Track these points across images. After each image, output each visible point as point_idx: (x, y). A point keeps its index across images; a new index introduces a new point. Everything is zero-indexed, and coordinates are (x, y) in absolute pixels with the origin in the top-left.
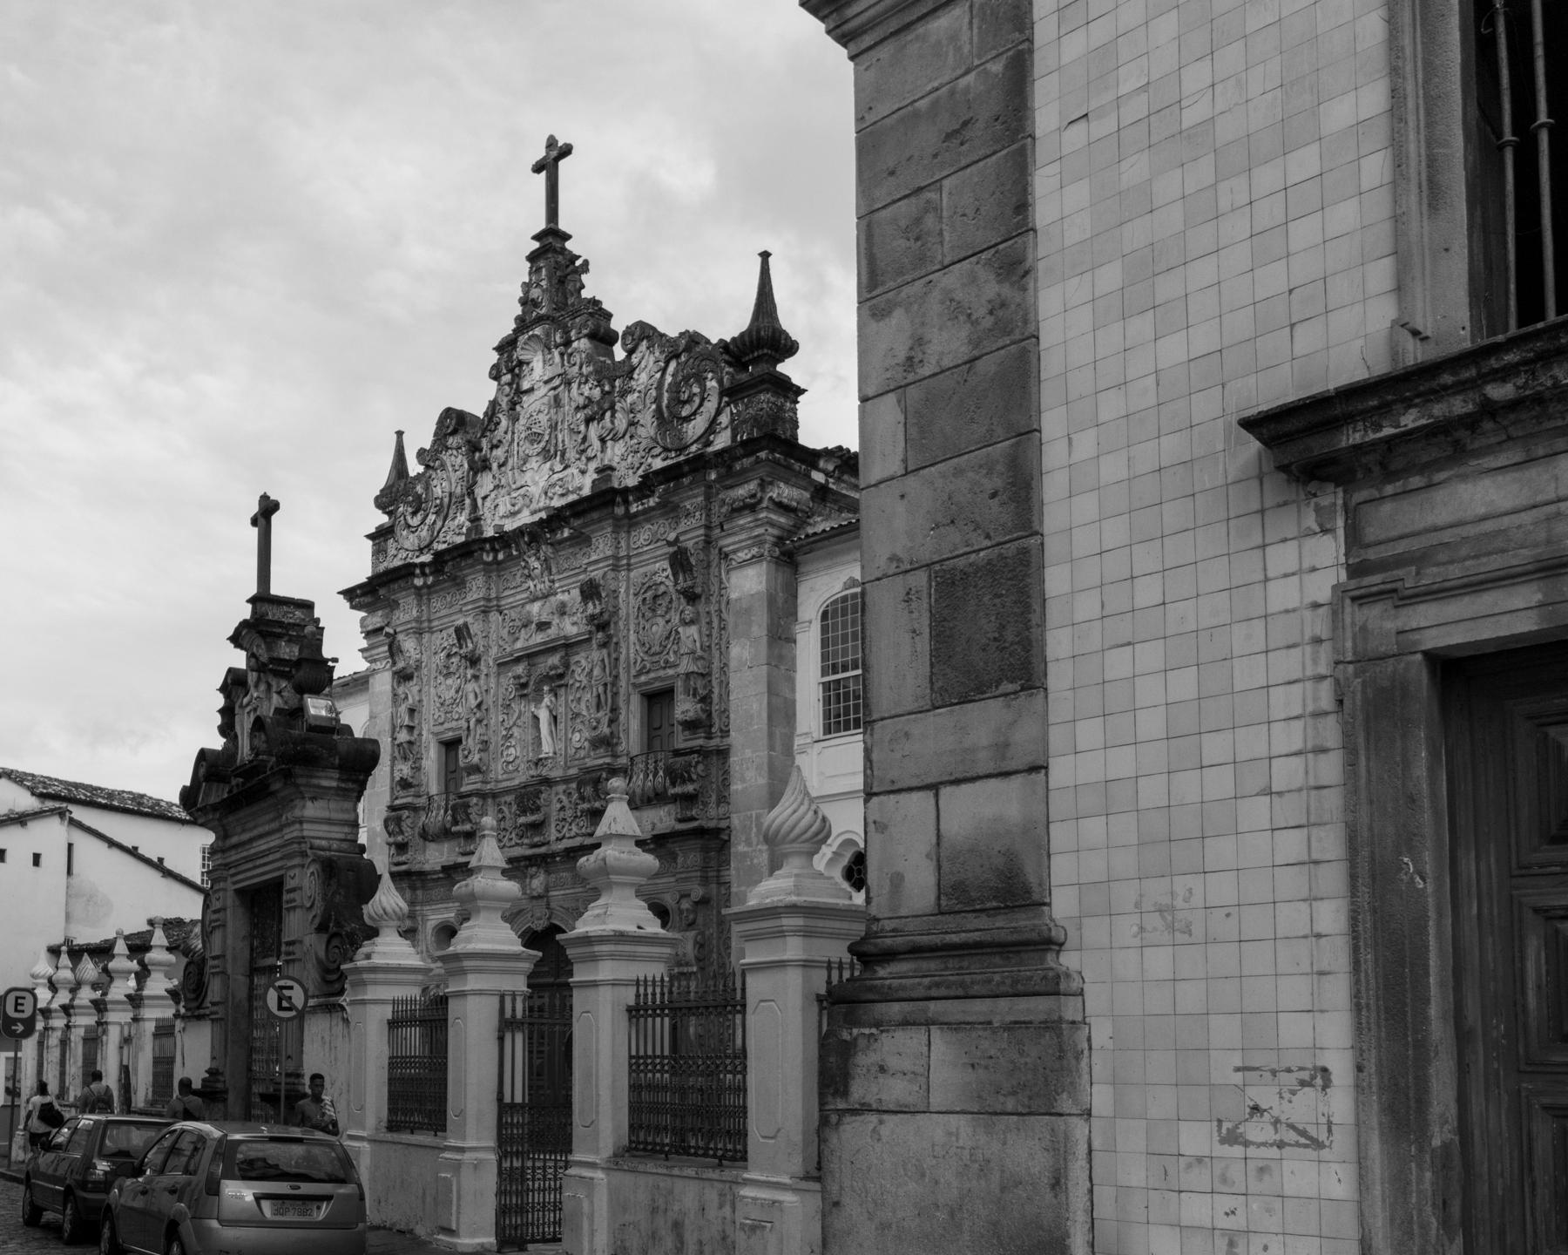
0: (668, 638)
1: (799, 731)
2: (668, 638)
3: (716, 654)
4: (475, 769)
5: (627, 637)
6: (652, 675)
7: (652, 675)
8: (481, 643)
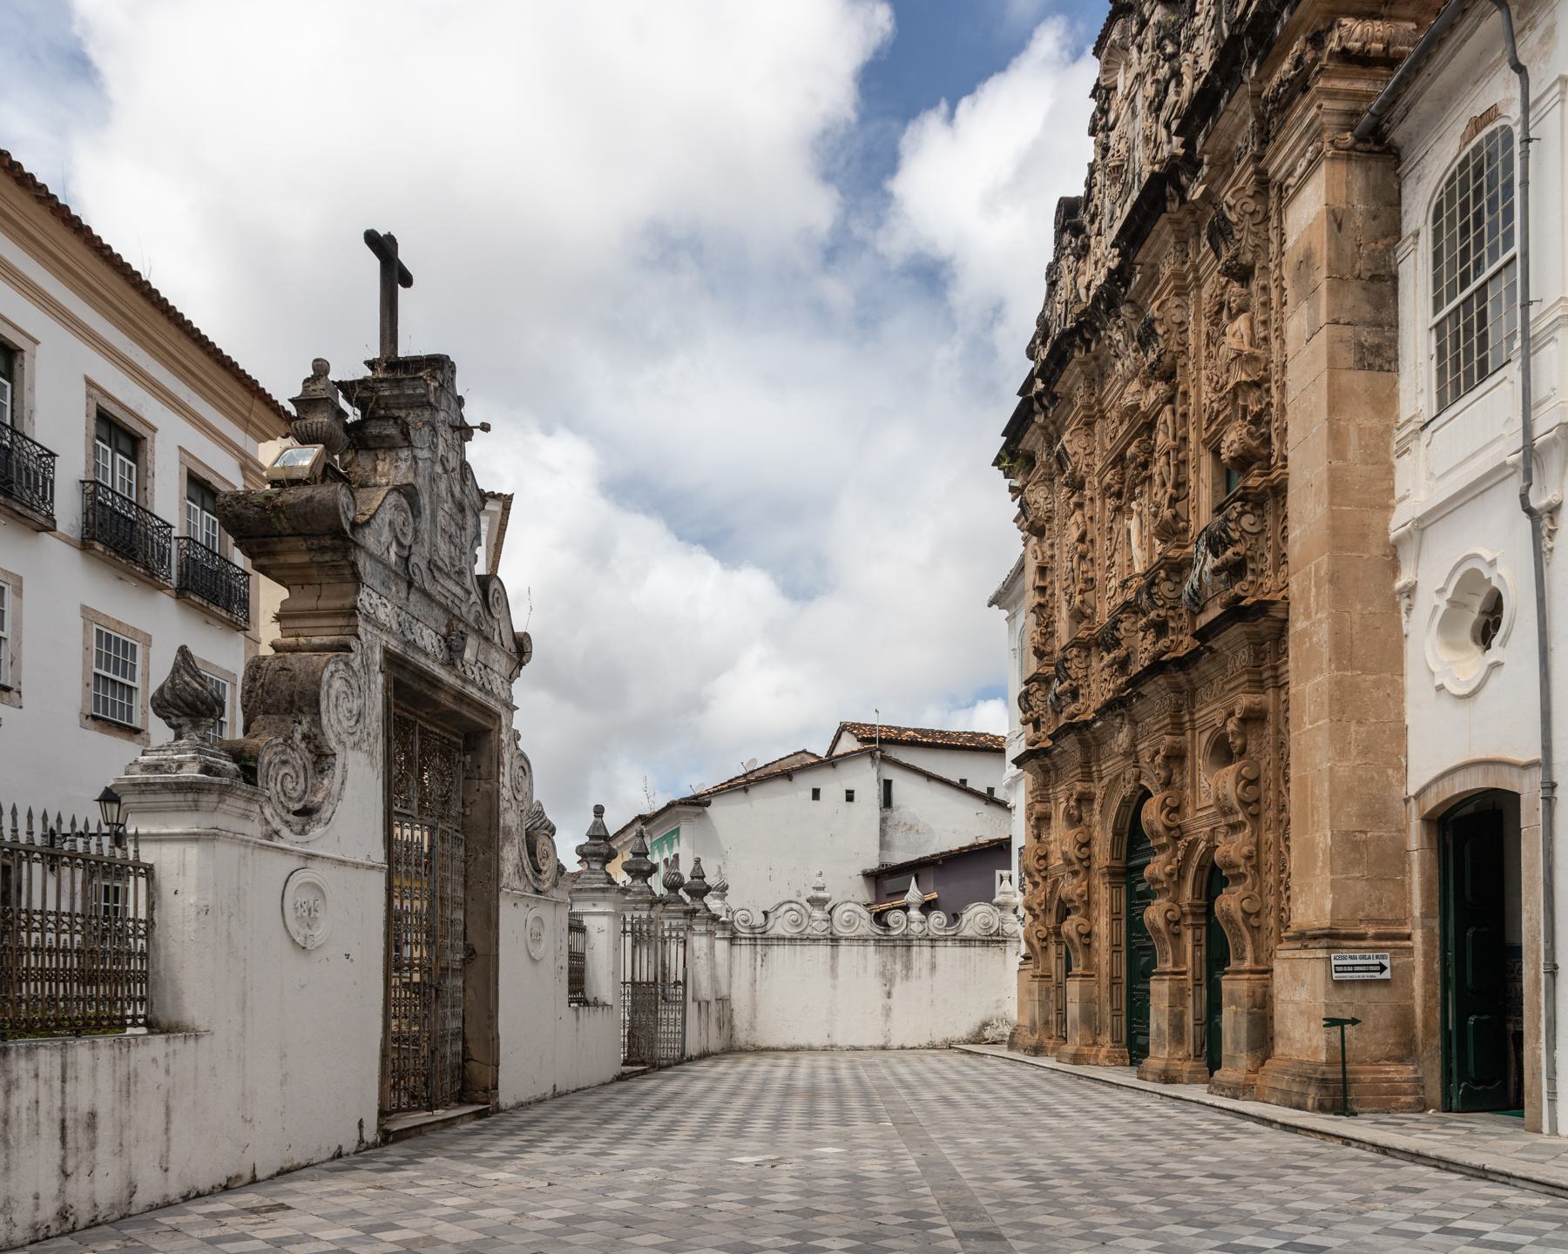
8: (1083, 462)
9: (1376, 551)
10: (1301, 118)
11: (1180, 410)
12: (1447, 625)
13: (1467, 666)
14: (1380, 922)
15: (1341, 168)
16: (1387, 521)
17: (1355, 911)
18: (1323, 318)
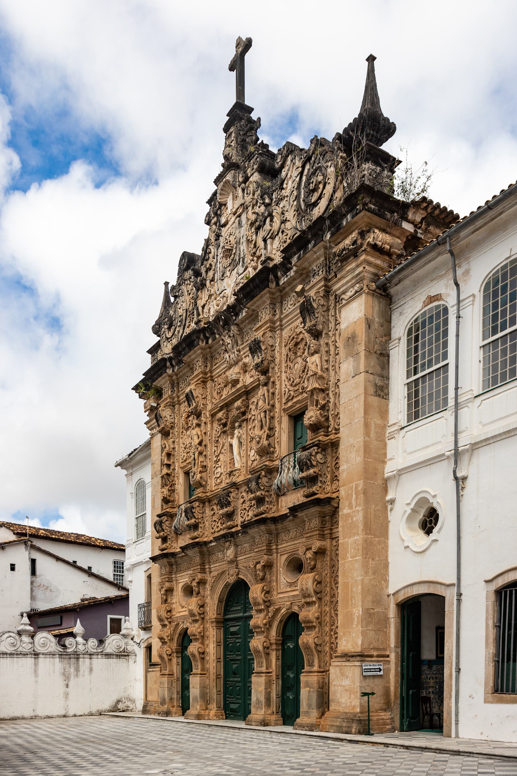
0: (303, 371)
1: (390, 423)
2: (303, 371)
3: (332, 373)
4: (199, 485)
5: (280, 377)
6: (295, 400)
7: (295, 400)
8: (201, 402)
9: (380, 482)
10: (354, 270)
11: (271, 391)
12: (410, 519)
13: (420, 539)
14: (378, 649)
15: (370, 298)
16: (384, 468)
17: (369, 645)
18: (362, 368)
